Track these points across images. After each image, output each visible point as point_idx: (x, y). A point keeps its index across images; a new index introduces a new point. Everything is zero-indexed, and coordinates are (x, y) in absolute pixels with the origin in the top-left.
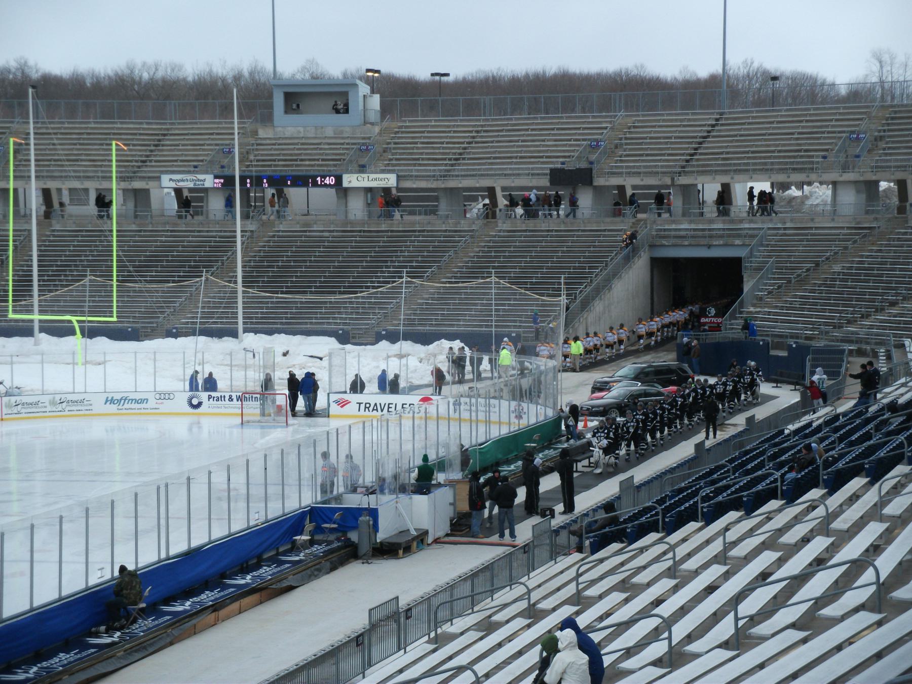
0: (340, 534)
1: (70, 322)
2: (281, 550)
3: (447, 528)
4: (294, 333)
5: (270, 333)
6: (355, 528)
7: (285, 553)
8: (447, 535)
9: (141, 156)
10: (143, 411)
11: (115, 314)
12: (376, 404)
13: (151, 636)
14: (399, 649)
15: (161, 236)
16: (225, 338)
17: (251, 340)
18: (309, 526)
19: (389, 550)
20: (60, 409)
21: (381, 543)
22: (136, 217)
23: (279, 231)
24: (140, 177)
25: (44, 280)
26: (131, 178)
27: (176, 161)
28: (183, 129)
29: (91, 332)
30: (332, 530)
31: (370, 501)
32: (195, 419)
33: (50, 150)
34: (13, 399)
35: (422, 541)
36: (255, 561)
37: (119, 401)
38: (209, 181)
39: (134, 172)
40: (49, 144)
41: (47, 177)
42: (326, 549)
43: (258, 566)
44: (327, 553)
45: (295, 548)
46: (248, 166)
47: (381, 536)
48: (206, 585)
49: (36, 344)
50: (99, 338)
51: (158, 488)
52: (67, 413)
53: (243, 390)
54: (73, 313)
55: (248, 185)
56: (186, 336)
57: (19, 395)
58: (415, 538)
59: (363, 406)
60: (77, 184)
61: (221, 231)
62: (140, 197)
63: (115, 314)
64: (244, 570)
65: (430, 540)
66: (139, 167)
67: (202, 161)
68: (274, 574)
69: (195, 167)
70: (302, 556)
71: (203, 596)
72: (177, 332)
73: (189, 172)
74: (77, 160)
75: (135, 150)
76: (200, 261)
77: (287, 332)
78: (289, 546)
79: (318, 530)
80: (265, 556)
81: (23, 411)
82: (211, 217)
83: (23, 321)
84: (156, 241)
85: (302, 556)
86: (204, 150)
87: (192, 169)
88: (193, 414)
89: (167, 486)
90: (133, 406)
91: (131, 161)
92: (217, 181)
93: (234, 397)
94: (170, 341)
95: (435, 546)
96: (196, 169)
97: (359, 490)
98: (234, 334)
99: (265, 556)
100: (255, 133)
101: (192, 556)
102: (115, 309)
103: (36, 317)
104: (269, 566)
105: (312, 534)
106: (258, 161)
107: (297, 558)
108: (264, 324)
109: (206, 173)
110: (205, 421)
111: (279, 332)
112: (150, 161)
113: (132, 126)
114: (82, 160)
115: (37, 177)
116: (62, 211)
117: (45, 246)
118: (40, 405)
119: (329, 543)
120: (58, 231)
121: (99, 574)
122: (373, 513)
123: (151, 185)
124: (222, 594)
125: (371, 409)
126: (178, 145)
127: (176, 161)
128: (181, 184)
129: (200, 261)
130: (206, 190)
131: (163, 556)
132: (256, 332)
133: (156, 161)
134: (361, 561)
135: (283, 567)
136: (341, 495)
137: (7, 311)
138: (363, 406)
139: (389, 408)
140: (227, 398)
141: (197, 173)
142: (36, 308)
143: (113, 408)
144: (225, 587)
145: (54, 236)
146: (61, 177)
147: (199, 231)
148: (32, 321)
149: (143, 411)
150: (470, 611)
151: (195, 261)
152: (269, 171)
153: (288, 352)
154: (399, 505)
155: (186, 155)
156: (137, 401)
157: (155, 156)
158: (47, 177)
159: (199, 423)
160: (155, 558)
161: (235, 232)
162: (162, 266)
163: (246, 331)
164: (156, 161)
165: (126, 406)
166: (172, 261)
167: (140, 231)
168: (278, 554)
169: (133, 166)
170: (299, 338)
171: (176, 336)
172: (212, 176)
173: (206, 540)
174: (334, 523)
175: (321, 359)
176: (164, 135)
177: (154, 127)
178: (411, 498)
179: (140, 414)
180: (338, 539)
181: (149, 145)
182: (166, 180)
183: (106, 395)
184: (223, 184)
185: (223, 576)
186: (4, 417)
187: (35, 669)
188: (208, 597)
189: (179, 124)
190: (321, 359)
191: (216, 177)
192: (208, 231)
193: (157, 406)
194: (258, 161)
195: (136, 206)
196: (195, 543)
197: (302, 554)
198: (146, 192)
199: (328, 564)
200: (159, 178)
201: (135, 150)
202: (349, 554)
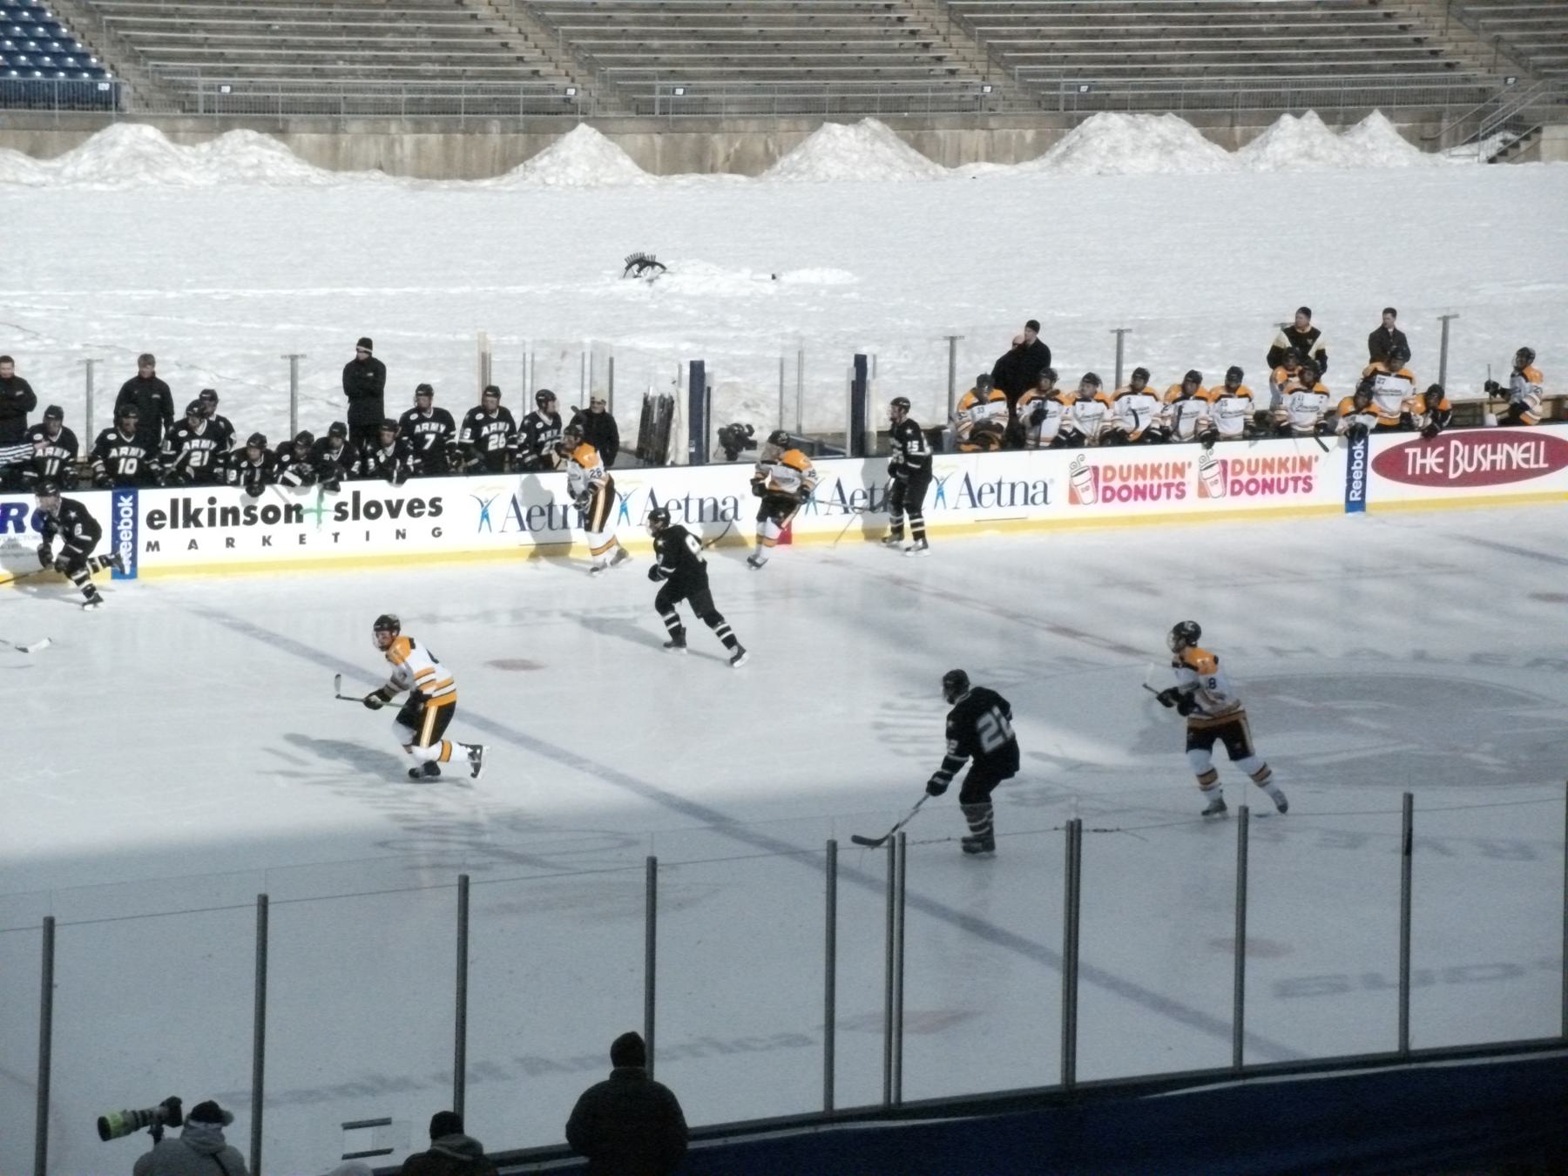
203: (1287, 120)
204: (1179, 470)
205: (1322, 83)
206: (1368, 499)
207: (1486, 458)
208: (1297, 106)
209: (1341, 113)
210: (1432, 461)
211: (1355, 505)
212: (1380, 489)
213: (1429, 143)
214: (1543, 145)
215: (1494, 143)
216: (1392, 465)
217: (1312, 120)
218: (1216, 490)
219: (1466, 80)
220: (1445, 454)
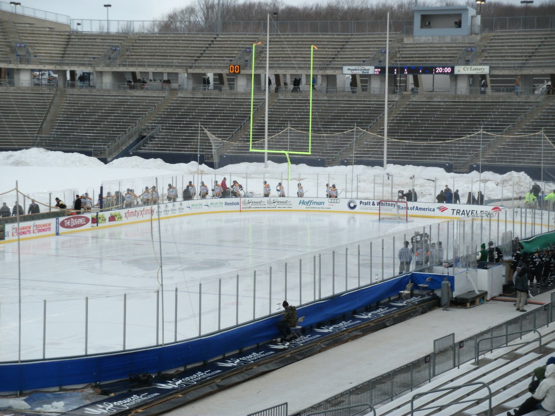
0: (430, 291)
1: (284, 154)
2: (392, 298)
4: (418, 165)
5: (403, 164)
6: (439, 287)
7: (394, 301)
8: (501, 295)
9: (332, 55)
10: (321, 209)
11: (310, 150)
12: (464, 211)
13: (307, 346)
14: (455, 367)
15: (342, 104)
16: (376, 167)
17: (391, 168)
18: (409, 286)
19: (460, 303)
20: (273, 206)
21: (456, 298)
22: (327, 92)
23: (413, 101)
24: (331, 68)
25: (272, 129)
26: (325, 68)
27: (353, 58)
28: (358, 38)
29: (296, 161)
30: (424, 289)
31: (450, 272)
32: (352, 215)
33: (280, 51)
34: (247, 199)
35: (483, 298)
36: (375, 304)
37: (307, 203)
38: (372, 70)
39: (328, 65)
40: (279, 48)
41: (277, 67)
42: (420, 300)
43: (377, 308)
44: (420, 302)
45: (400, 298)
46: (396, 61)
47: (455, 294)
48: (344, 317)
50: (301, 164)
51: (315, 257)
52: (277, 209)
53: (381, 199)
54: (286, 149)
55: (395, 73)
57: (252, 197)
58: (478, 296)
59: (455, 212)
62: (331, 80)
63: (310, 150)
64: (368, 309)
65: (488, 298)
66: (330, 61)
67: (368, 58)
68: (386, 313)
69: (364, 61)
70: (404, 303)
71: (341, 324)
72: (347, 162)
73: (360, 65)
75: (329, 51)
76: (363, 119)
78: (397, 297)
79: (416, 287)
80: (382, 302)
81: (253, 206)
82: (372, 92)
83: (259, 153)
84: (338, 107)
85: (404, 303)
86: (370, 51)
87: (362, 63)
88: (351, 212)
89: (320, 256)
90: (316, 206)
92: (376, 70)
93: (376, 203)
94: (343, 167)
95: (491, 302)
96: (364, 63)
97: (444, 264)
98: (381, 164)
99: (382, 302)
100: (402, 40)
101: (335, 300)
102: (310, 147)
103: (266, 151)
104: (383, 308)
105: (412, 290)
106: (402, 58)
107: (401, 305)
108: (401, 158)
109: (371, 65)
110: (358, 217)
111: (409, 164)
112: (338, 58)
113: (328, 36)
114: (298, 57)
115: (269, 67)
116: (285, 88)
117: (274, 109)
118: (262, 203)
119: (423, 296)
120: (282, 100)
121: (278, 307)
122: (451, 279)
123: (337, 72)
124: (352, 323)
125: (460, 213)
126: (354, 48)
127: (353, 58)
128: (355, 72)
129: (363, 119)
130: (370, 76)
131: (317, 298)
132: (395, 163)
133: (341, 58)
134: (442, 308)
135: (392, 310)
138: (455, 212)
139: (472, 213)
140: (371, 203)
141: (365, 65)
142: (266, 146)
143: (304, 207)
144: (355, 319)
145: (279, 103)
146: (285, 67)
147: (364, 101)
148: (264, 153)
150: (505, 345)
151: (361, 119)
152: (409, 64)
154: (468, 275)
155: (359, 54)
156: (318, 203)
157: (341, 54)
158: (277, 67)
159: (353, 218)
160: (312, 300)
161: (384, 101)
162: (341, 122)
163: (388, 162)
164: (341, 58)
165: (311, 206)
166: (347, 119)
167: (329, 100)
168: (390, 301)
169: (327, 61)
170: (421, 168)
171: (346, 164)
172: (373, 67)
173: (344, 290)
174: (426, 284)
176: (347, 42)
177: (341, 37)
178: (476, 271)
179: (320, 211)
180: (428, 294)
181: (337, 48)
182: (345, 68)
184: (380, 72)
185: (355, 312)
186: (242, 209)
187: (238, 361)
188: (343, 325)
189: (356, 35)
191: (376, 68)
192: (369, 101)
193: (330, 207)
194: (402, 58)
195: (327, 85)
196: (337, 292)
197: (405, 302)
198: (334, 77)
199: (421, 309)
200: (342, 68)
201: (329, 51)
202: (434, 303)
204: (30, 227)
206: (60, 232)
207: (74, 222)
211: (57, 234)
212: (62, 230)
216: (63, 224)
218: (36, 231)
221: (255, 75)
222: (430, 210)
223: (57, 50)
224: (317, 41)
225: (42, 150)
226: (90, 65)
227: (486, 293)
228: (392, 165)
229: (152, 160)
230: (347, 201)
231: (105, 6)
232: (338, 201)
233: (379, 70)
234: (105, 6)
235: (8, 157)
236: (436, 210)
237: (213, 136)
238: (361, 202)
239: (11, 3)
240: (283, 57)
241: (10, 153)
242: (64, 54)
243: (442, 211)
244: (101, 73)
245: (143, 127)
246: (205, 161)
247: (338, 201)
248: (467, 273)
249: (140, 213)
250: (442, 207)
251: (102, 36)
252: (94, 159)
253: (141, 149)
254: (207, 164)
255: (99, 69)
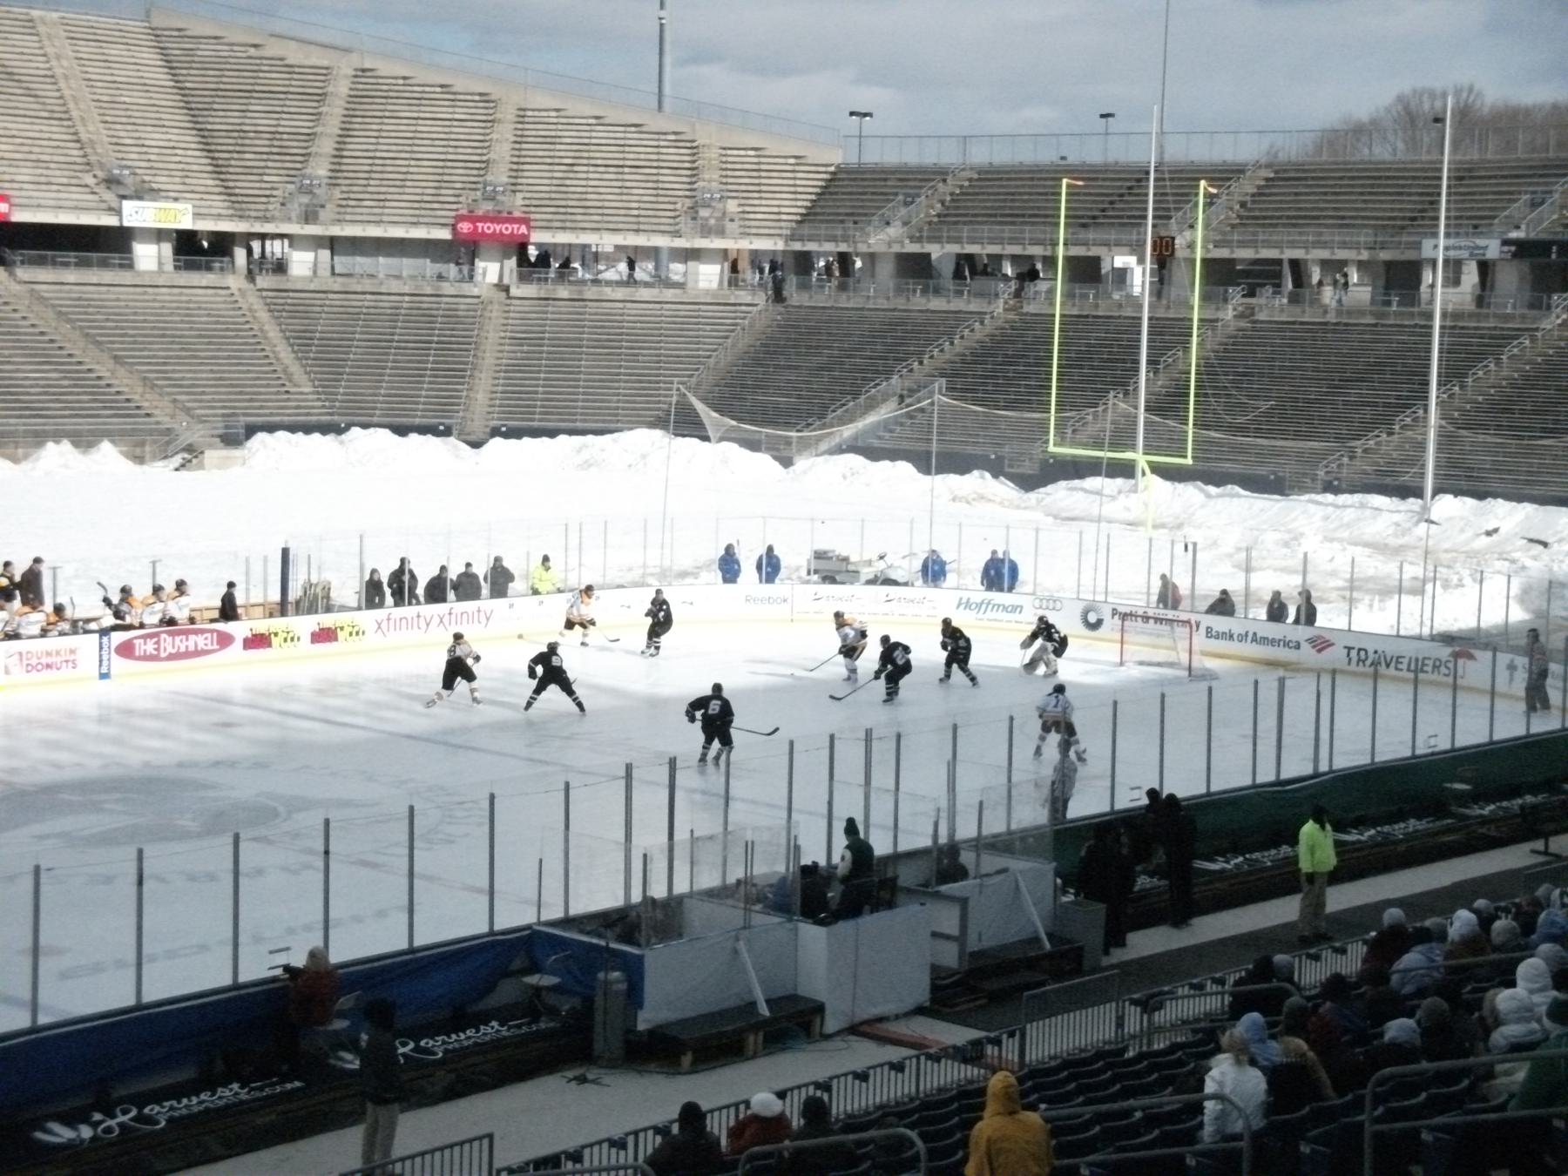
3: (920, 993)
4: (1520, 499)
5: (1480, 495)
8: (920, 1011)
9: (1412, 210)
17: (1448, 506)
21: (651, 1033)
38: (1493, 249)
47: (645, 1020)
49: (1134, 490)
55: (1554, 256)
56: (1352, 492)
59: (1354, 653)
60: (1325, 254)
61: (1495, 328)
66: (1403, 228)
69: (1476, 227)
74: (1318, 218)
77: (1508, 497)
91: (1394, 218)
92: (1506, 248)
98: (1418, 493)
108: (1466, 480)
111: (1495, 496)
112: (1423, 218)
114: (1325, 217)
125: (1368, 662)
132: (1458, 492)
136: (680, 900)
137: (1047, 442)
138: (1354, 653)
149: (1014, 626)
153: (1496, 530)
154: (742, 945)
156: (1005, 608)
163: (1436, 492)
165: (989, 614)
167: (1376, 325)
170: (1528, 508)
172: (1498, 242)
175: (1545, 545)
183: (960, 593)
190: (1545, 545)
203: (50, 446)
205: (70, 424)
207: (182, 644)
208: (57, 436)
209: (84, 441)
210: (150, 647)
212: (119, 664)
213: (139, 460)
214: (206, 461)
215: (177, 460)
216: (126, 650)
217: (66, 445)
219: (158, 423)
220: (158, 643)
221: (1067, 259)
222: (1287, 644)
223: (792, 208)
224: (1388, 178)
225: (657, 434)
226: (845, 239)
227: (819, 1009)
228: (1449, 497)
229: (887, 463)
230: (1081, 606)
231: (1103, 116)
232: (1058, 605)
233: (1513, 248)
234: (1103, 116)
235: (579, 451)
236: (1305, 647)
237: (715, 415)
238: (1114, 612)
239: (852, 114)
240: (1288, 217)
241: (590, 437)
242: (809, 216)
243: (1319, 651)
244: (871, 258)
245: (907, 384)
246: (1007, 470)
247: (1058, 605)
248: (737, 939)
249: (436, 620)
250: (1319, 637)
251: (901, 172)
252: (764, 460)
253: (880, 438)
254: (1012, 478)
255: (862, 248)
